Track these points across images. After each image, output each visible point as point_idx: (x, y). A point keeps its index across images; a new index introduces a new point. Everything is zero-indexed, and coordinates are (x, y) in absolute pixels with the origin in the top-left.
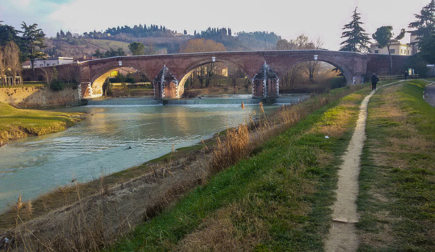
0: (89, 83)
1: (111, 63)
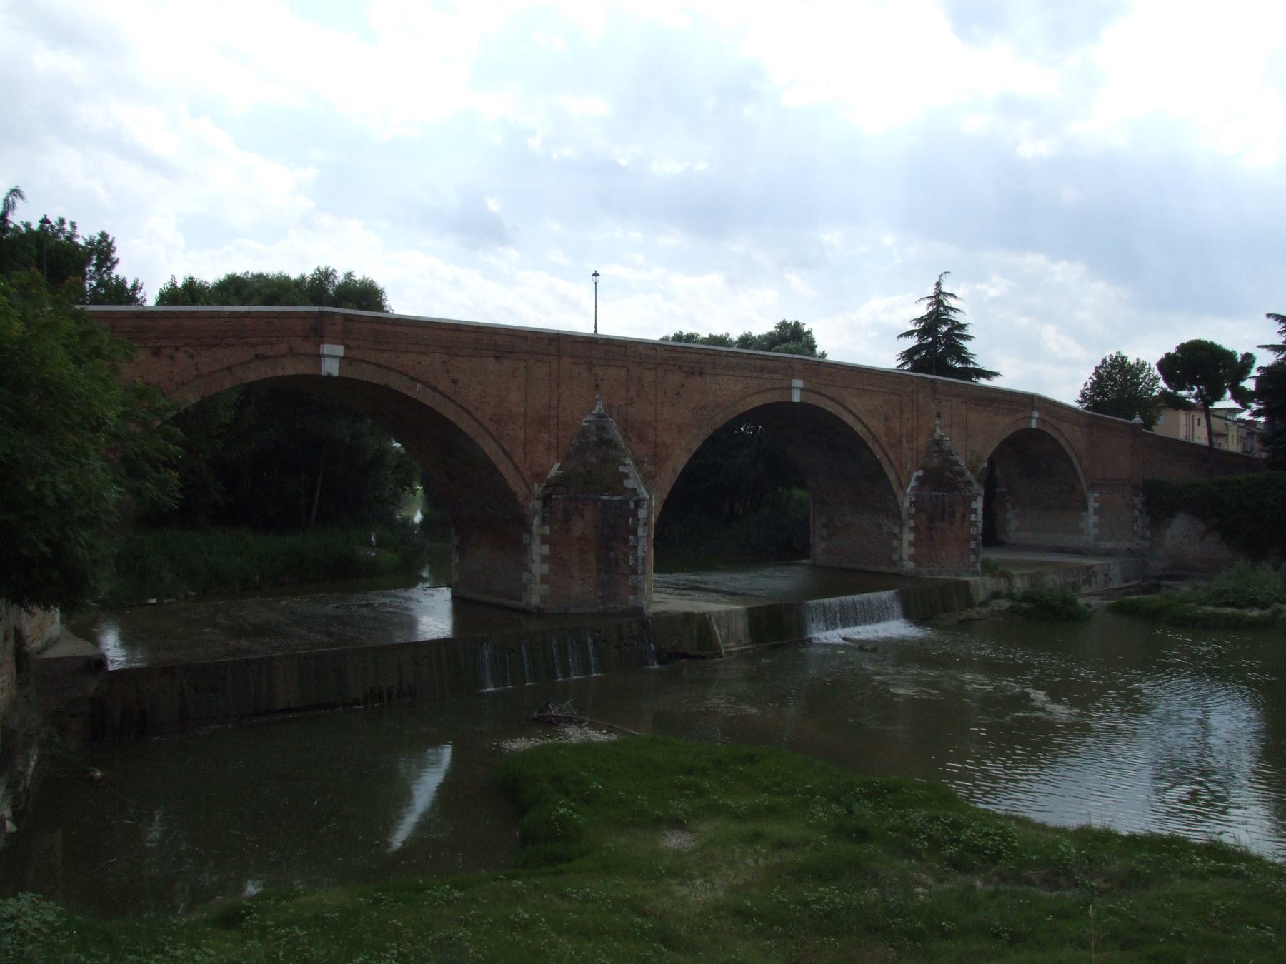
1: (261, 350)
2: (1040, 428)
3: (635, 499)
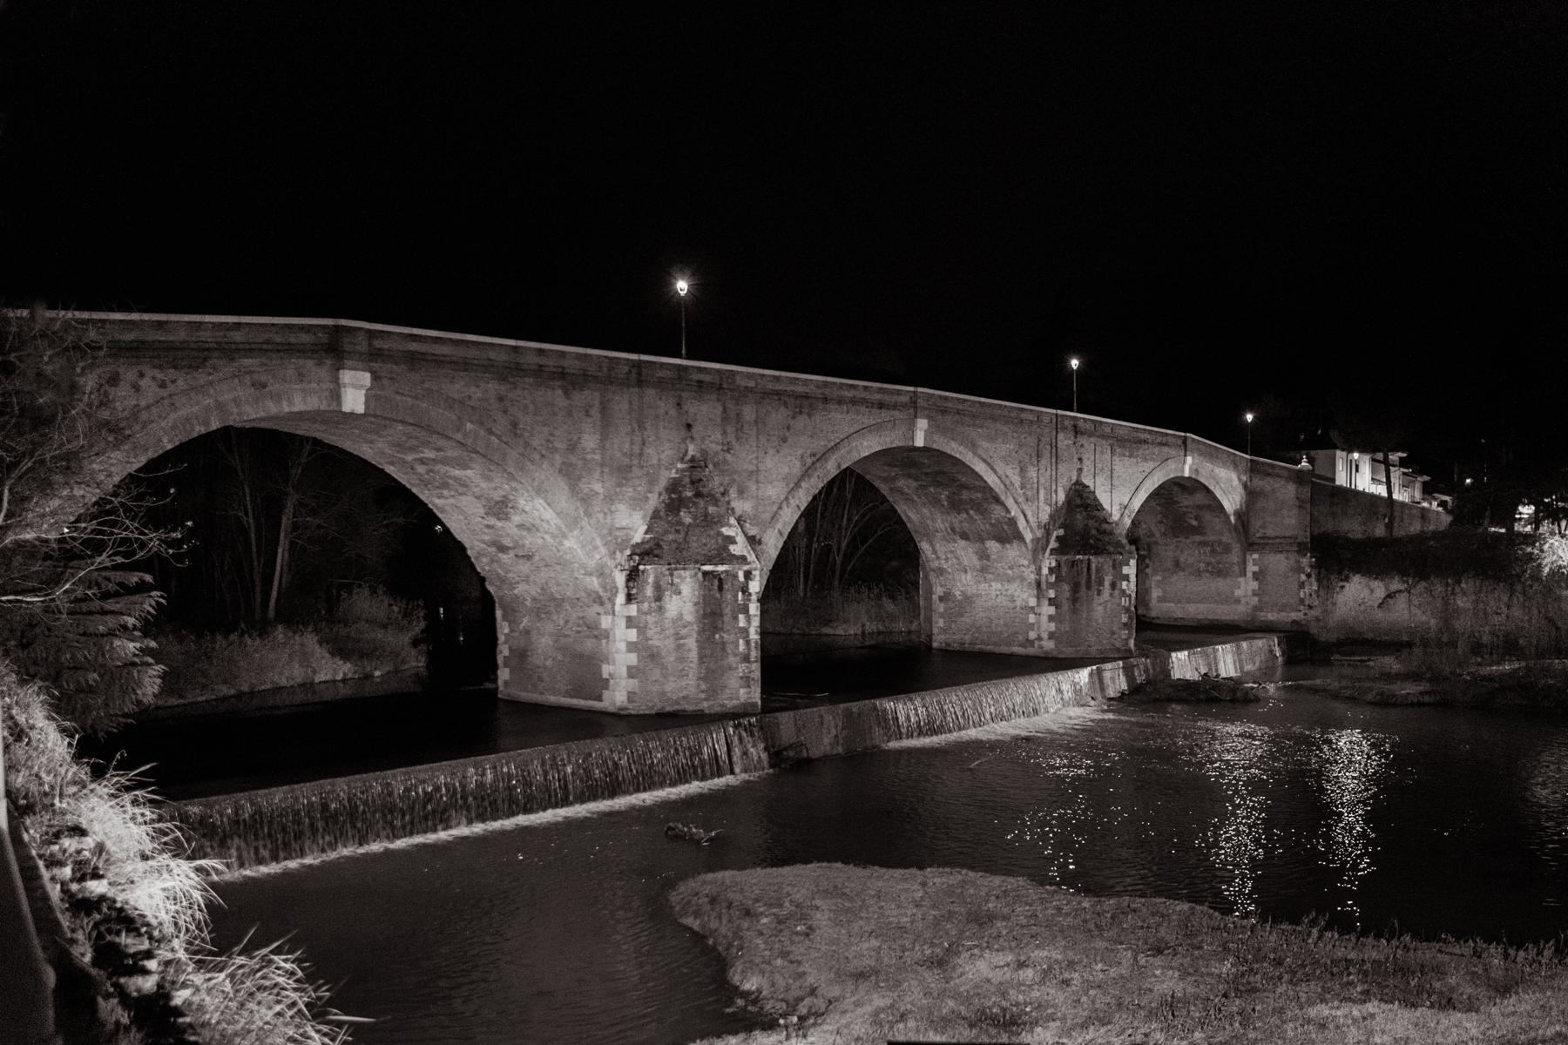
2: (1193, 476)
3: (746, 568)
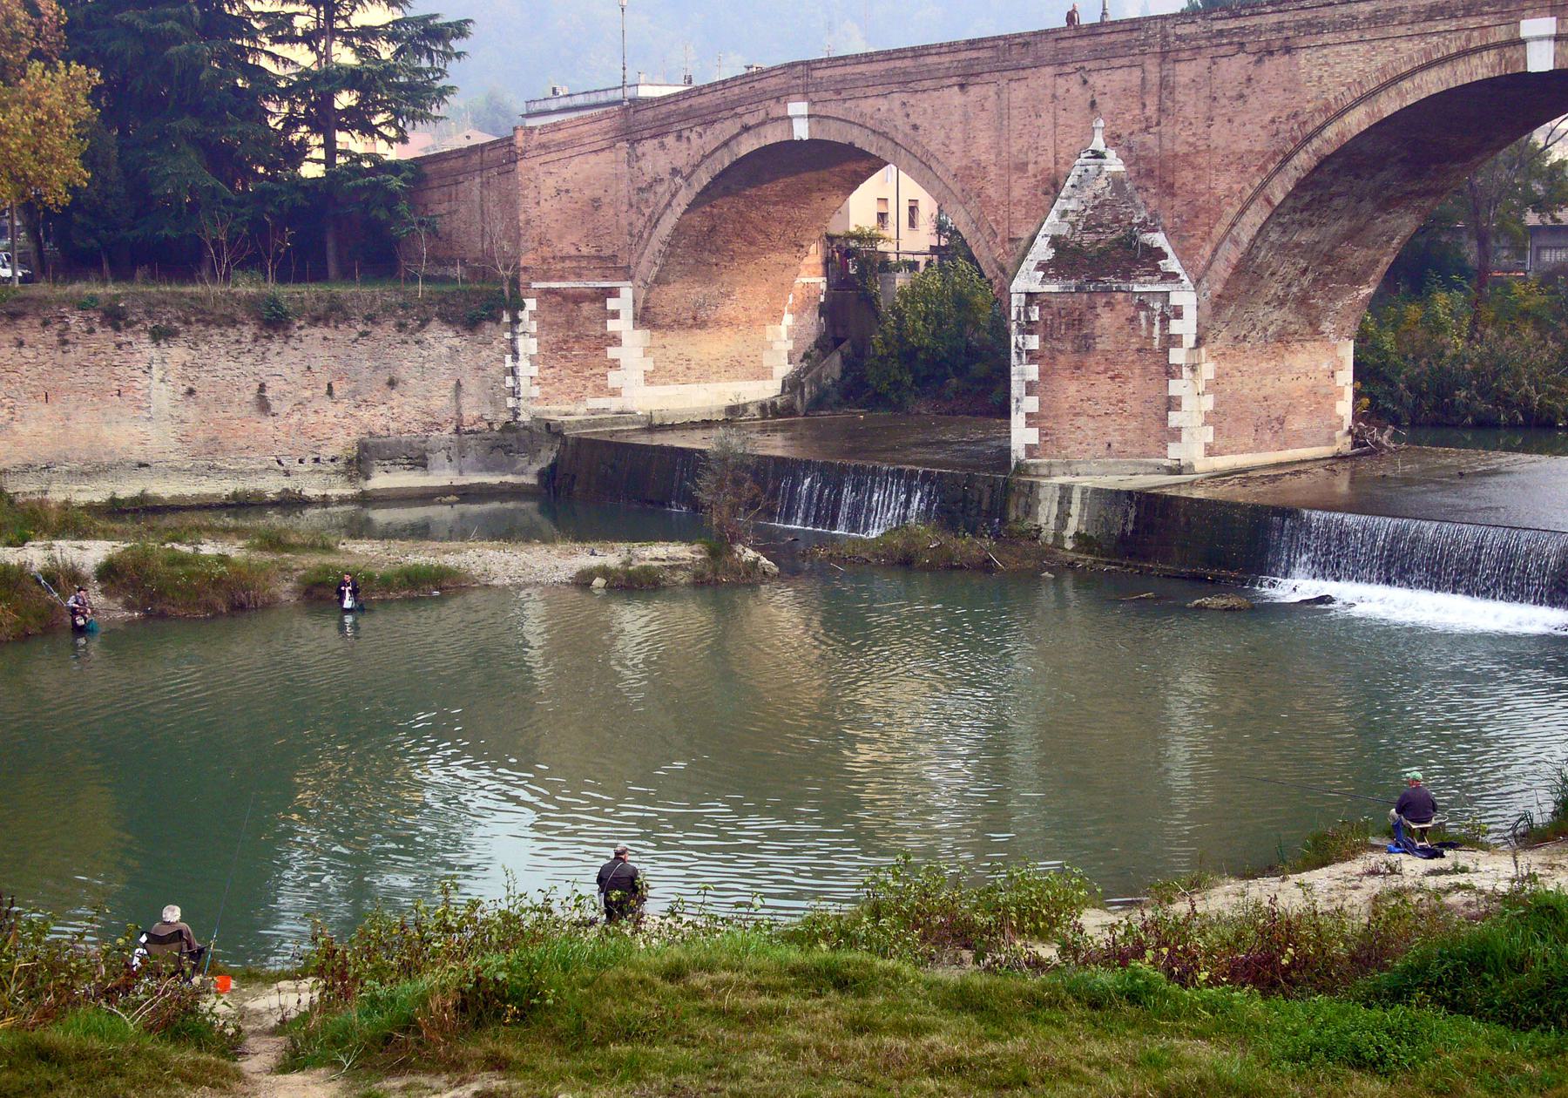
0: (613, 293)
